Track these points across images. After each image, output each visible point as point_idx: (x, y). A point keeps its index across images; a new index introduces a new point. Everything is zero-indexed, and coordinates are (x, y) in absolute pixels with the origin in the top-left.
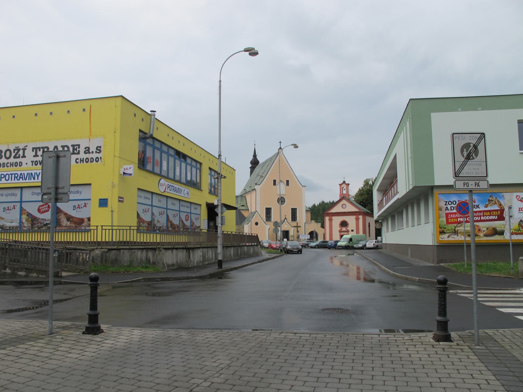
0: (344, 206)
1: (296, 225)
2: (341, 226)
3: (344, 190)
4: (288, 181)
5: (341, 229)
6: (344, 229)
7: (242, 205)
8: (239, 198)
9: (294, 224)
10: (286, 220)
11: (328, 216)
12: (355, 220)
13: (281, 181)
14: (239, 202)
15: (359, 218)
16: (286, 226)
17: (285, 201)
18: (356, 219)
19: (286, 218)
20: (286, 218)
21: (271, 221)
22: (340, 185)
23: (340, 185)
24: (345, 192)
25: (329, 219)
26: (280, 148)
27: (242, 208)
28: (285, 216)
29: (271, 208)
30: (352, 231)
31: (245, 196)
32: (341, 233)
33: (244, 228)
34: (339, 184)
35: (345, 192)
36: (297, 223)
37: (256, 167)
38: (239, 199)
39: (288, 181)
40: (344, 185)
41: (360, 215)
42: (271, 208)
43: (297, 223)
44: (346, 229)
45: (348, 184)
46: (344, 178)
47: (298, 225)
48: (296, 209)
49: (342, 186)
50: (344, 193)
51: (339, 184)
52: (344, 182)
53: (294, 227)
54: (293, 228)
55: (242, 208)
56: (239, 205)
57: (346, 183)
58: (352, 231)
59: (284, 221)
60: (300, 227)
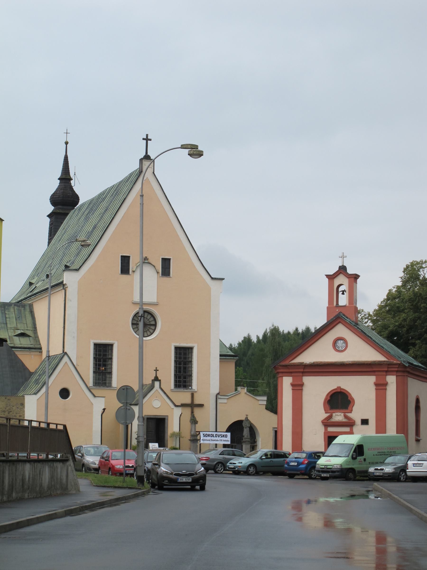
0: (340, 343)
1: (188, 401)
2: (328, 406)
3: (340, 294)
4: (166, 263)
5: (330, 417)
6: (338, 417)
7: (19, 332)
8: (12, 310)
10: (157, 384)
11: (288, 374)
12: (373, 388)
13: (145, 261)
15: (386, 384)
16: (157, 404)
17: (155, 325)
18: (376, 384)
22: (331, 278)
23: (331, 278)
24: (343, 300)
25: (292, 385)
26: (147, 157)
27: (18, 342)
28: (156, 370)
29: (111, 345)
30: (365, 422)
31: (31, 306)
32: (330, 429)
33: (23, 405)
34: (327, 276)
35: (343, 300)
37: (67, 214)
39: (166, 263)
40: (341, 279)
41: (388, 372)
42: (111, 345)
44: (346, 417)
45: (356, 277)
46: (343, 257)
47: (197, 402)
48: (191, 349)
49: (337, 282)
50: (341, 304)
51: (327, 276)
52: (343, 269)
53: (183, 405)
54: (178, 412)
55: (18, 342)
56: (11, 333)
57: (350, 271)
58: (365, 422)
59: (152, 387)
60: (201, 406)
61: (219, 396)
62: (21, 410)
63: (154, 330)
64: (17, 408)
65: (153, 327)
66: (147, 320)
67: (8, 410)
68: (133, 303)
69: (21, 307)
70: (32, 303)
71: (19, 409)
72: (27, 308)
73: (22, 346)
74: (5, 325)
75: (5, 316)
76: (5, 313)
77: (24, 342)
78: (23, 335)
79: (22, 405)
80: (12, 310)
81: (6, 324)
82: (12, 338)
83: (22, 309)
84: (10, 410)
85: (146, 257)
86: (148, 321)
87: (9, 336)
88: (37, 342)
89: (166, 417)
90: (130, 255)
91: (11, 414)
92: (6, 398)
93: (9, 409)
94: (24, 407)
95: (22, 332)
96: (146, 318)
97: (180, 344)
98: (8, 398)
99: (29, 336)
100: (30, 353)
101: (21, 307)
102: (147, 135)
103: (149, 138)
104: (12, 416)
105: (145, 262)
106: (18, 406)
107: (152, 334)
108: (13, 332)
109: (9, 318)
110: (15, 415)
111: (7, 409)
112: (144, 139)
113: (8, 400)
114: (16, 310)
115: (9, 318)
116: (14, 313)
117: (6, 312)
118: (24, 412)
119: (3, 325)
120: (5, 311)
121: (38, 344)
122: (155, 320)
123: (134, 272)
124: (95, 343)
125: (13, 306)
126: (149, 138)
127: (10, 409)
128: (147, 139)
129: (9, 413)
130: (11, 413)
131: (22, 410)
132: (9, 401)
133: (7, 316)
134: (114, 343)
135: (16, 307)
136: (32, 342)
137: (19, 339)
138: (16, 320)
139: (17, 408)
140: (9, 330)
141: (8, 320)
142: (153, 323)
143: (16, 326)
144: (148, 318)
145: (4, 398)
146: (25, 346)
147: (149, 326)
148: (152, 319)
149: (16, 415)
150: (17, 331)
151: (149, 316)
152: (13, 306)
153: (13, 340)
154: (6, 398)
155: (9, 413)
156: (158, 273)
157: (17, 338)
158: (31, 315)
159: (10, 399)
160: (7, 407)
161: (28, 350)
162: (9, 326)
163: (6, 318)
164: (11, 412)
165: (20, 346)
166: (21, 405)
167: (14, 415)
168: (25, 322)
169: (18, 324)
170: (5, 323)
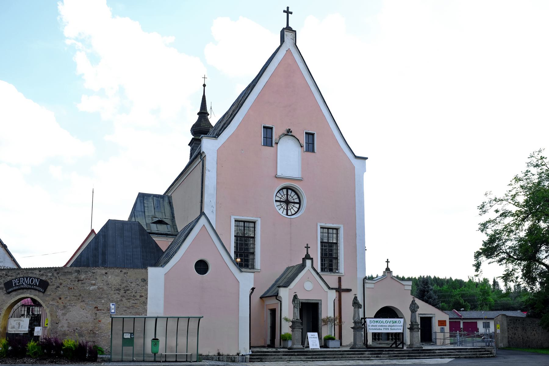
7: (157, 219)
8: (151, 200)
9: (331, 279)
13: (289, 133)
14: (150, 211)
16: (308, 286)
17: (299, 203)
19: (308, 257)
20: (308, 257)
21: (253, 268)
27: (154, 228)
36: (340, 279)
38: (150, 204)
43: (340, 279)
55: (154, 228)
56: (149, 221)
61: (367, 281)
62: (142, 288)
63: (299, 209)
64: (137, 285)
65: (297, 206)
66: (291, 197)
67: (125, 288)
68: (276, 177)
69: (160, 198)
70: (171, 194)
71: (139, 287)
72: (166, 200)
73: (159, 232)
74: (143, 213)
75: (144, 205)
76: (144, 202)
77: (162, 228)
78: (160, 222)
79: (144, 282)
80: (151, 200)
81: (144, 212)
82: (150, 225)
83: (161, 199)
84: (127, 288)
85: (290, 129)
86: (292, 199)
87: (146, 223)
88: (174, 229)
89: (319, 302)
90: (272, 126)
91: (129, 294)
92: (121, 271)
93: (125, 286)
94: (147, 284)
95: (160, 219)
96: (290, 196)
97: (326, 224)
98: (124, 271)
99: (167, 224)
100: (167, 239)
101: (160, 198)
102: (288, 8)
103: (289, 11)
104: (130, 296)
105: (289, 134)
106: (138, 283)
107: (296, 213)
108: (151, 220)
109: (148, 207)
110: (134, 295)
111: (123, 286)
112: (284, 11)
113: (125, 273)
114: (155, 201)
115: (148, 207)
116: (152, 203)
117: (145, 202)
118: (147, 290)
119: (141, 213)
120: (144, 201)
121: (176, 231)
122: (299, 198)
123: (277, 143)
124: (236, 219)
125: (152, 196)
126: (289, 11)
127: (128, 287)
128: (288, 12)
129: (125, 293)
130: (128, 292)
131: (144, 288)
132: (125, 275)
133: (146, 205)
134: (257, 220)
135: (155, 198)
136: (170, 229)
137: (157, 226)
138: (154, 209)
139: (137, 285)
140: (146, 218)
141: (146, 208)
142: (297, 201)
143: (154, 214)
144: (292, 195)
145: (119, 271)
146: (162, 232)
147: (293, 204)
148: (296, 197)
149: (135, 295)
150: (155, 219)
151: (293, 194)
152: (152, 196)
153: (150, 227)
154: (121, 271)
155: (125, 293)
156: (301, 146)
157: (155, 225)
158: (169, 205)
159: (128, 273)
160: (123, 283)
161: (165, 236)
162: (147, 214)
163: (144, 207)
164: (129, 290)
165: (157, 232)
166: (142, 281)
167: (133, 295)
168: (163, 212)
169: (156, 213)
170: (143, 211)
